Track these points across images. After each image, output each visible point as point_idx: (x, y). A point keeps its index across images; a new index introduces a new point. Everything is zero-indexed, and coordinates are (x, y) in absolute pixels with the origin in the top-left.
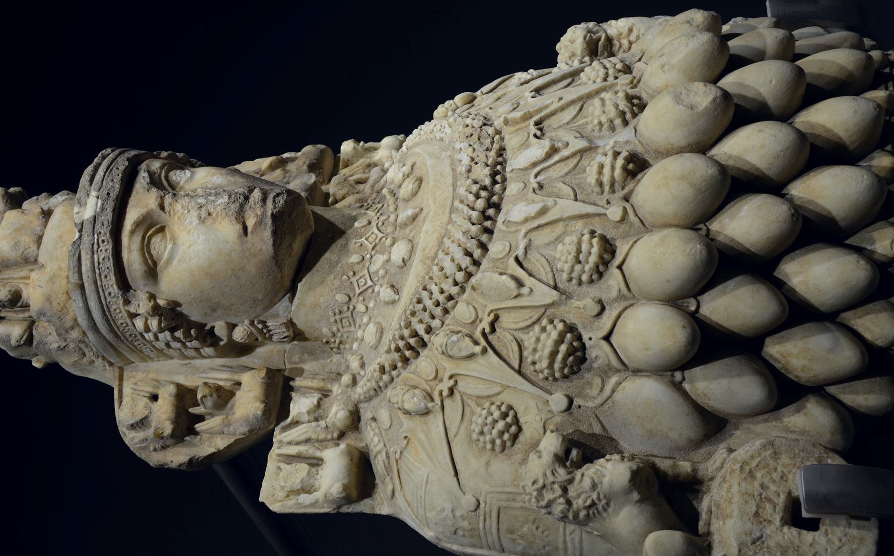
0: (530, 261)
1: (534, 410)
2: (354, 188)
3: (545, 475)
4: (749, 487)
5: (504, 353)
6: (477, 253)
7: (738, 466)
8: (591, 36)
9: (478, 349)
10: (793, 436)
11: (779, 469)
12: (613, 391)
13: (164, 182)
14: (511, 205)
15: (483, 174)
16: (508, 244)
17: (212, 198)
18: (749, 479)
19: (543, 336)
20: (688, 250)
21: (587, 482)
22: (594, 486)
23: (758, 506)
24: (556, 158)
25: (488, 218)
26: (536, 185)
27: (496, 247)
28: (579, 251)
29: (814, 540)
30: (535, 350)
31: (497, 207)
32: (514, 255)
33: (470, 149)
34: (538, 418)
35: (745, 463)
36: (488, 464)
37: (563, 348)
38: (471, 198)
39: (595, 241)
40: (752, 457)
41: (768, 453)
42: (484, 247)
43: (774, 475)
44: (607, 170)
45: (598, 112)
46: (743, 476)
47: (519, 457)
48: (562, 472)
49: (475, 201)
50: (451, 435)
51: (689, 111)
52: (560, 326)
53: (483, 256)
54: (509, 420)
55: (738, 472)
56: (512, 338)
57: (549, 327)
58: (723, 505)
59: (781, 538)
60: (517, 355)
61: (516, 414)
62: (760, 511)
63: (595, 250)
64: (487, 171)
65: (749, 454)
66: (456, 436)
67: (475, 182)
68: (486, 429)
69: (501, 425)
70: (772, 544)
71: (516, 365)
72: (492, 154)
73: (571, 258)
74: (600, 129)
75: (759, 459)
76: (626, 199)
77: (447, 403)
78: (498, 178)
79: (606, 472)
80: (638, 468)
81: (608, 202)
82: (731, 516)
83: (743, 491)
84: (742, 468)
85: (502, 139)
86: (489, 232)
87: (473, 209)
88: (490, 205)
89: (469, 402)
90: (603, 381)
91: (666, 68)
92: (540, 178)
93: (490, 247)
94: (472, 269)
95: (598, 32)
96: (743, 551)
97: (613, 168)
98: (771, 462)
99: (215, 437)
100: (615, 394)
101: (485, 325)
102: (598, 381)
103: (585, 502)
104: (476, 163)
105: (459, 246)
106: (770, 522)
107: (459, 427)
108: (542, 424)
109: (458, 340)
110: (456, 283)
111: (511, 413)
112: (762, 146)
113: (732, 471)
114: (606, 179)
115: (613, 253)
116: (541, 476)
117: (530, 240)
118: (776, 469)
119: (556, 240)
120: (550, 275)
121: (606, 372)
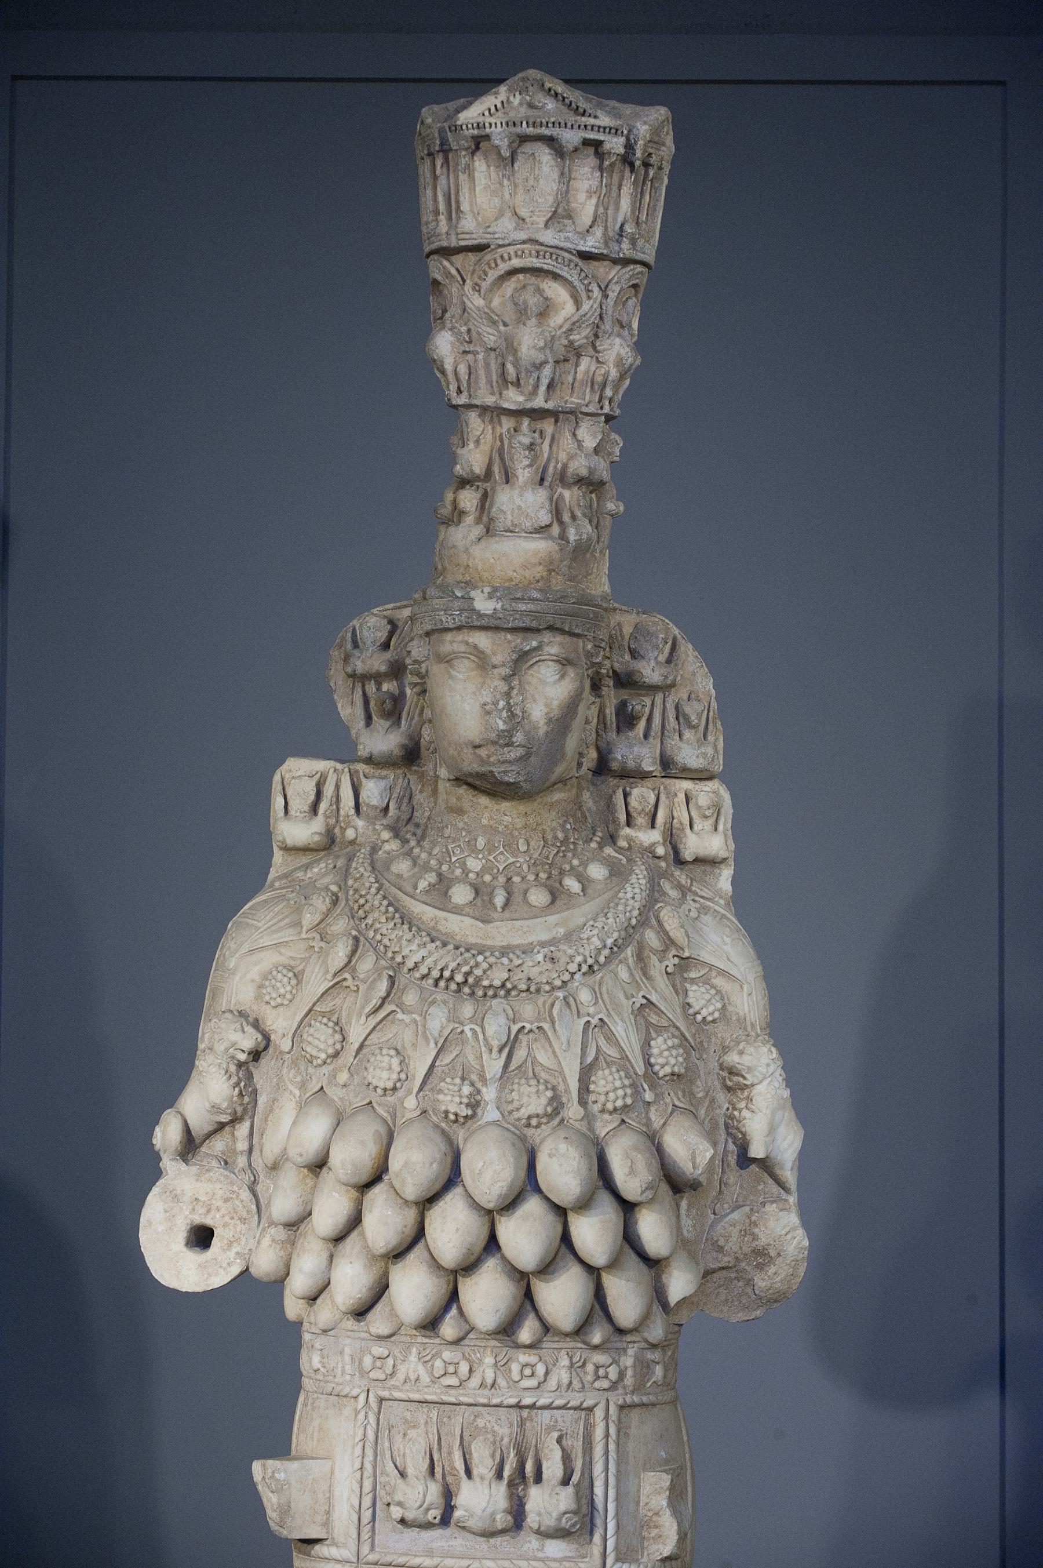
2: (640, 814)
13: (537, 659)
17: (504, 714)
38: (465, 969)
54: (279, 1000)
63: (381, 1085)
64: (497, 983)
99: (349, 709)
101: (350, 982)
118: (232, 1218)
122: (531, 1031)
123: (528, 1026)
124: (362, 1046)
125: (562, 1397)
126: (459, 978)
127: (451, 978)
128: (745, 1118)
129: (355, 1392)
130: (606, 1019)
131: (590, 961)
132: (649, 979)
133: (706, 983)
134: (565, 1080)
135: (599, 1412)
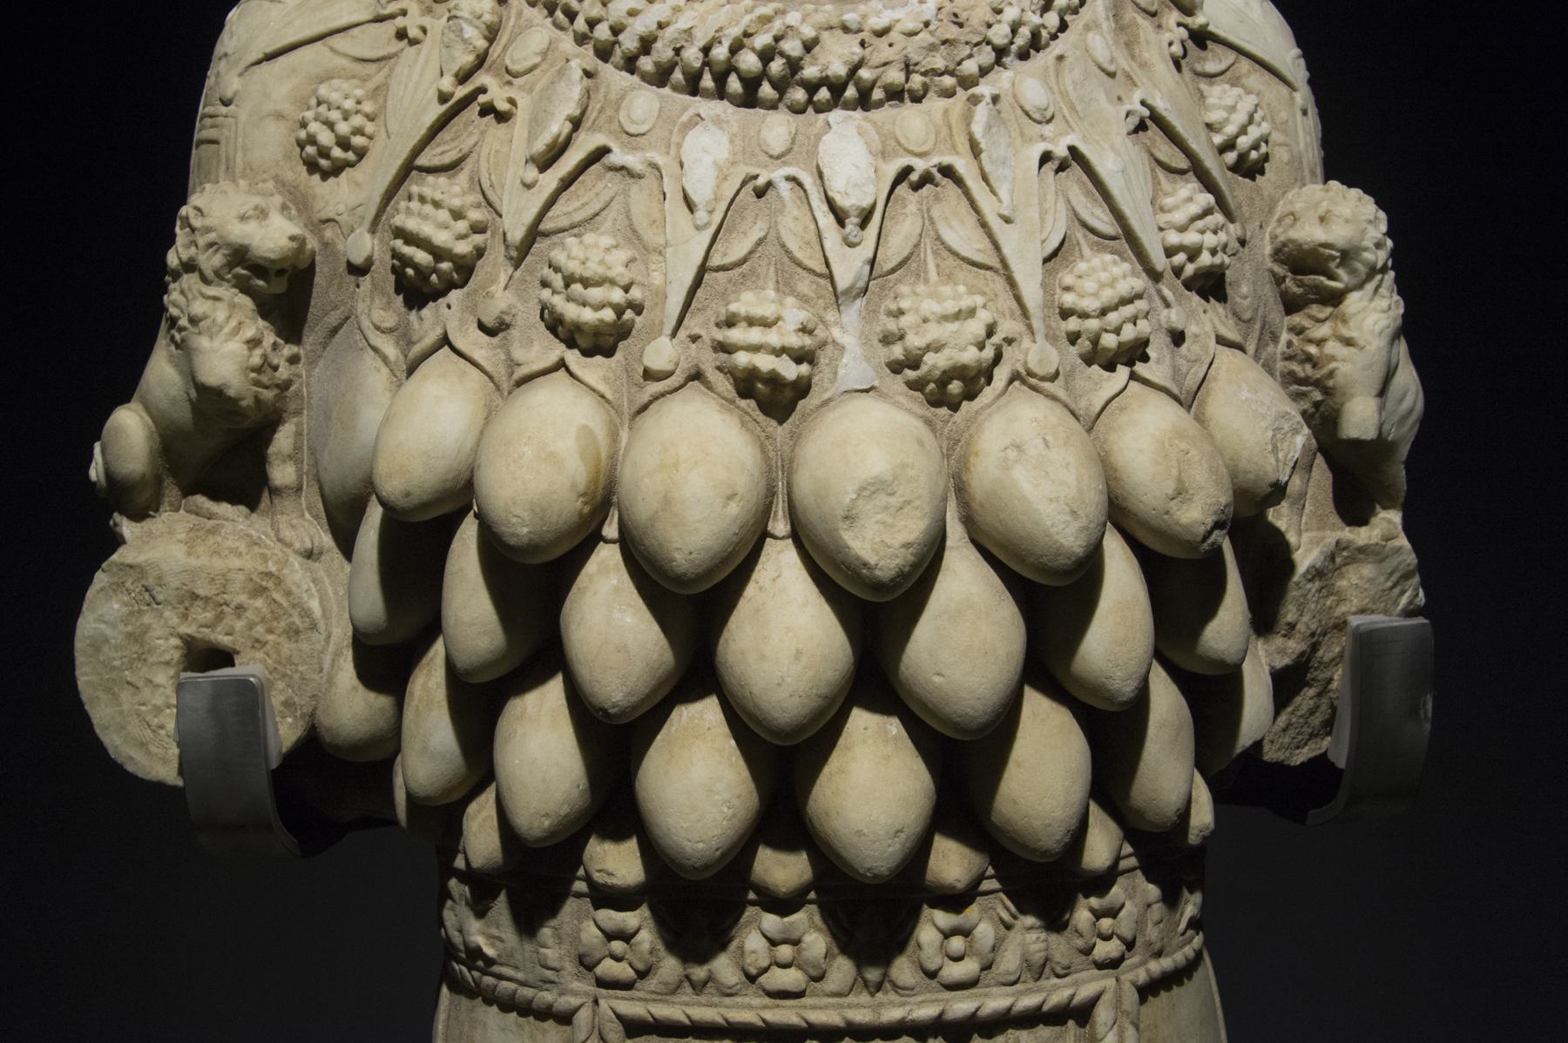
0: (600, 177)
1: (353, 200)
3: (208, 230)
4: (237, 586)
5: (445, 135)
6: (646, 64)
7: (272, 568)
8: (1334, 258)
9: (447, 83)
10: (326, 666)
11: (271, 637)
12: (375, 349)
14: (735, 129)
15: (834, 59)
16: (643, 129)
18: (250, 586)
19: (443, 215)
20: (518, 511)
21: (199, 307)
22: (194, 321)
23: (207, 599)
24: (826, 220)
25: (721, 79)
26: (761, 181)
27: (644, 103)
28: (586, 283)
29: (159, 686)
30: (422, 199)
31: (749, 100)
32: (612, 145)
33: (911, 25)
34: (341, 208)
35: (279, 581)
36: (279, 116)
37: (422, 257)
38: (762, 40)
39: (608, 315)
40: (288, 593)
41: (297, 620)
42: (661, 77)
43: (260, 629)
44: (755, 335)
45: (930, 307)
46: (254, 577)
47: (289, 176)
48: (218, 260)
49: (753, 50)
50: (336, 41)
51: (840, 512)
52: (463, 248)
53: (647, 79)
54: (337, 152)
55: (261, 568)
56: (465, 150)
57: (462, 226)
58: (211, 540)
59: (158, 633)
60: (437, 161)
61: (351, 165)
62: (199, 603)
63: (588, 316)
64: (839, 69)
65: (294, 588)
66: (332, 49)
67: (809, 46)
68: (322, 109)
69: (326, 138)
70: (147, 619)
71: (422, 160)
72: (895, 76)
73: (573, 267)
74: (890, 314)
75: (285, 604)
76: (697, 376)
77: (389, 28)
78: (824, 94)
79: (216, 343)
80: (234, 401)
81: (695, 339)
82: (189, 554)
83: (231, 575)
84: (269, 575)
85: (949, 94)
86: (692, 86)
87: (735, 49)
88: (751, 84)
89: (386, 71)
90: (391, 331)
91: (1012, 454)
92: (785, 188)
93: (667, 90)
94: (618, 55)
95: (1353, 272)
96: (132, 572)
97: (755, 349)
98: (283, 624)
100: (372, 353)
101: (498, 95)
102: (389, 320)
103: (176, 305)
104: (862, 44)
105: (661, 26)
106: (185, 617)
107: (345, 55)
108: (331, 215)
109: (465, 41)
110: (592, 23)
111: (351, 156)
112: (763, 657)
113: (265, 558)
114: (736, 335)
115: (587, 353)
116: (208, 222)
117: (640, 177)
118: (270, 631)
119: (634, 231)
120: (564, 222)
121: (404, 337)
122: (927, 179)
123: (920, 165)
124: (534, 233)
125: (1029, 991)
126: (749, 61)
127: (730, 68)
128: (1332, 358)
129: (565, 1002)
130: (1084, 149)
131: (1036, 19)
132: (1143, 65)
133: (1235, 83)
134: (1011, 283)
135: (1103, 1014)
